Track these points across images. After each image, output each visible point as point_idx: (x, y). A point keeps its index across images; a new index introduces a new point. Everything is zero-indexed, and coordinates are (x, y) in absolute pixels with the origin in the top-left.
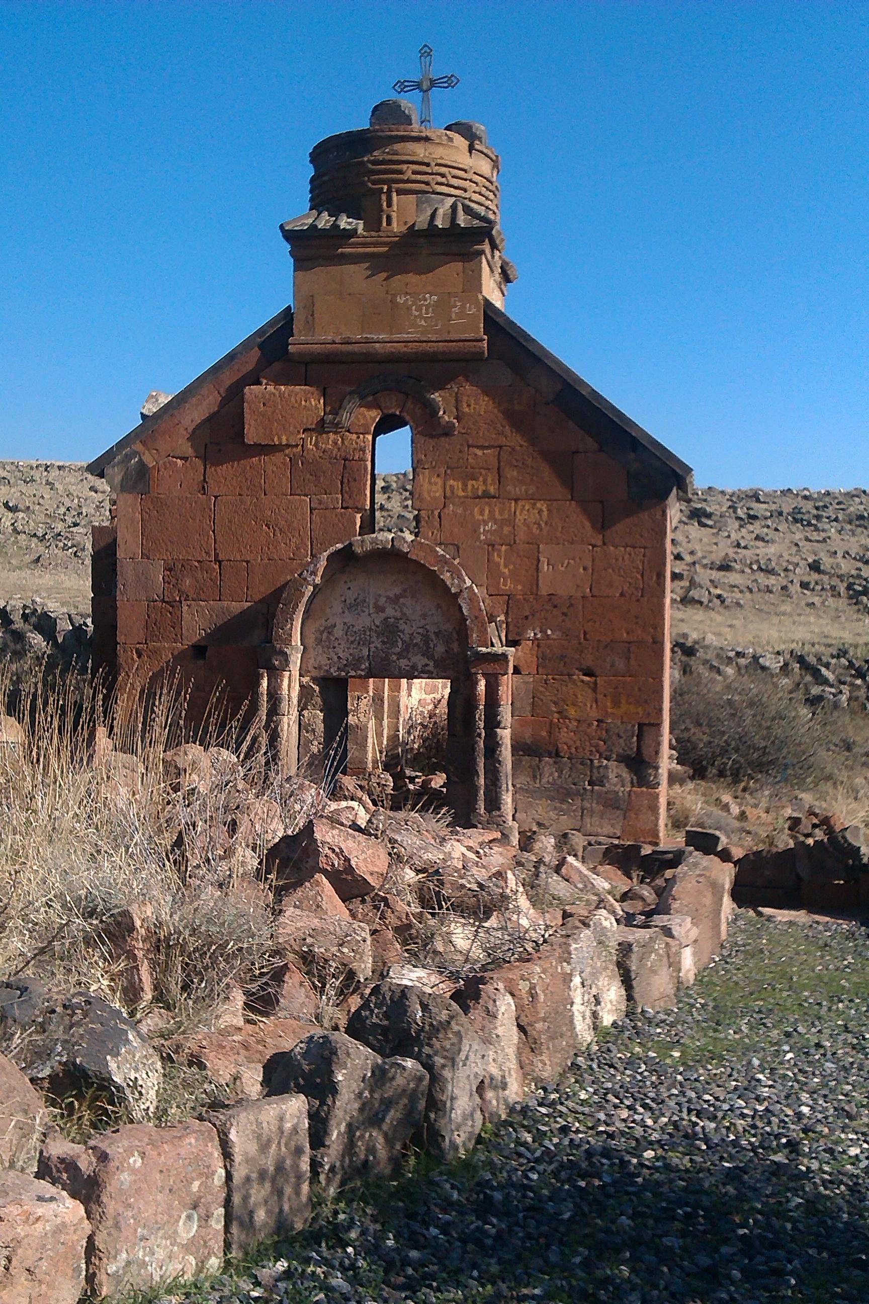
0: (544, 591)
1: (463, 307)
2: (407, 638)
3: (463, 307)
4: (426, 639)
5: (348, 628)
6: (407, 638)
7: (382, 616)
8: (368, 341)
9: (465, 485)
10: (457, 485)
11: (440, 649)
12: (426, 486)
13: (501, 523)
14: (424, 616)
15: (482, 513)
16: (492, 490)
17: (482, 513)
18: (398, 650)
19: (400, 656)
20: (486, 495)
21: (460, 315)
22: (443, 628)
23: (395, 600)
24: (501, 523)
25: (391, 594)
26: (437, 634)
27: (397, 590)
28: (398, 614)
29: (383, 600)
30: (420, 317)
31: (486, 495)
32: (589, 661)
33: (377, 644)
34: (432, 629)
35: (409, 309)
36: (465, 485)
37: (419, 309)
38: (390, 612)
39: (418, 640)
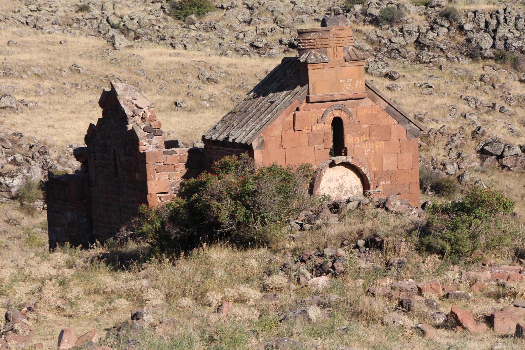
0: (384, 169)
1: (359, 82)
2: (346, 189)
3: (359, 82)
4: (352, 189)
5: (328, 187)
6: (346, 189)
7: (338, 183)
8: (332, 95)
9: (360, 138)
10: (358, 138)
11: (355, 192)
12: (349, 140)
13: (371, 149)
14: (351, 181)
15: (365, 147)
16: (368, 139)
17: (365, 147)
18: (343, 193)
19: (344, 195)
20: (366, 140)
21: (358, 85)
22: (356, 184)
23: (342, 177)
24: (371, 149)
25: (340, 175)
26: (354, 187)
27: (342, 174)
28: (343, 182)
29: (338, 178)
30: (347, 86)
31: (366, 140)
32: (399, 190)
33: (337, 192)
34: (353, 185)
35: (343, 84)
36: (360, 138)
37: (346, 84)
38: (340, 181)
39: (349, 189)
